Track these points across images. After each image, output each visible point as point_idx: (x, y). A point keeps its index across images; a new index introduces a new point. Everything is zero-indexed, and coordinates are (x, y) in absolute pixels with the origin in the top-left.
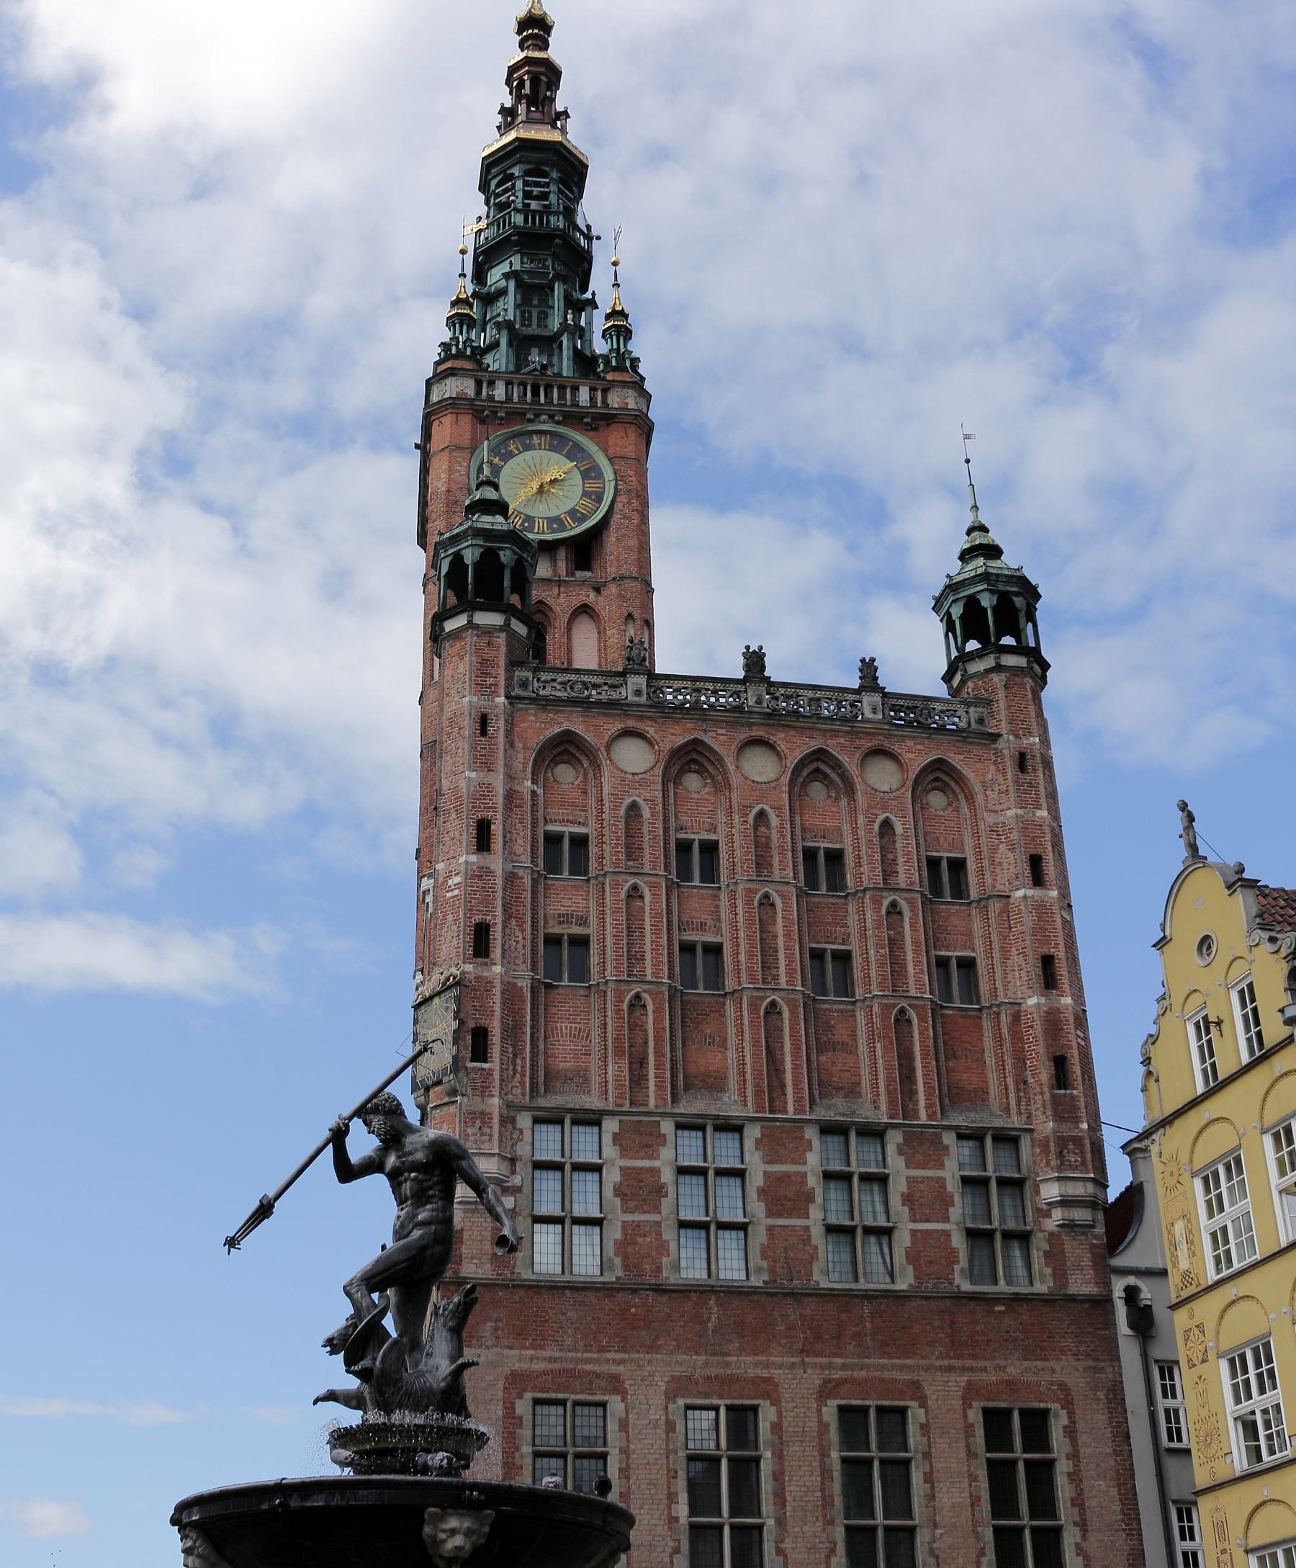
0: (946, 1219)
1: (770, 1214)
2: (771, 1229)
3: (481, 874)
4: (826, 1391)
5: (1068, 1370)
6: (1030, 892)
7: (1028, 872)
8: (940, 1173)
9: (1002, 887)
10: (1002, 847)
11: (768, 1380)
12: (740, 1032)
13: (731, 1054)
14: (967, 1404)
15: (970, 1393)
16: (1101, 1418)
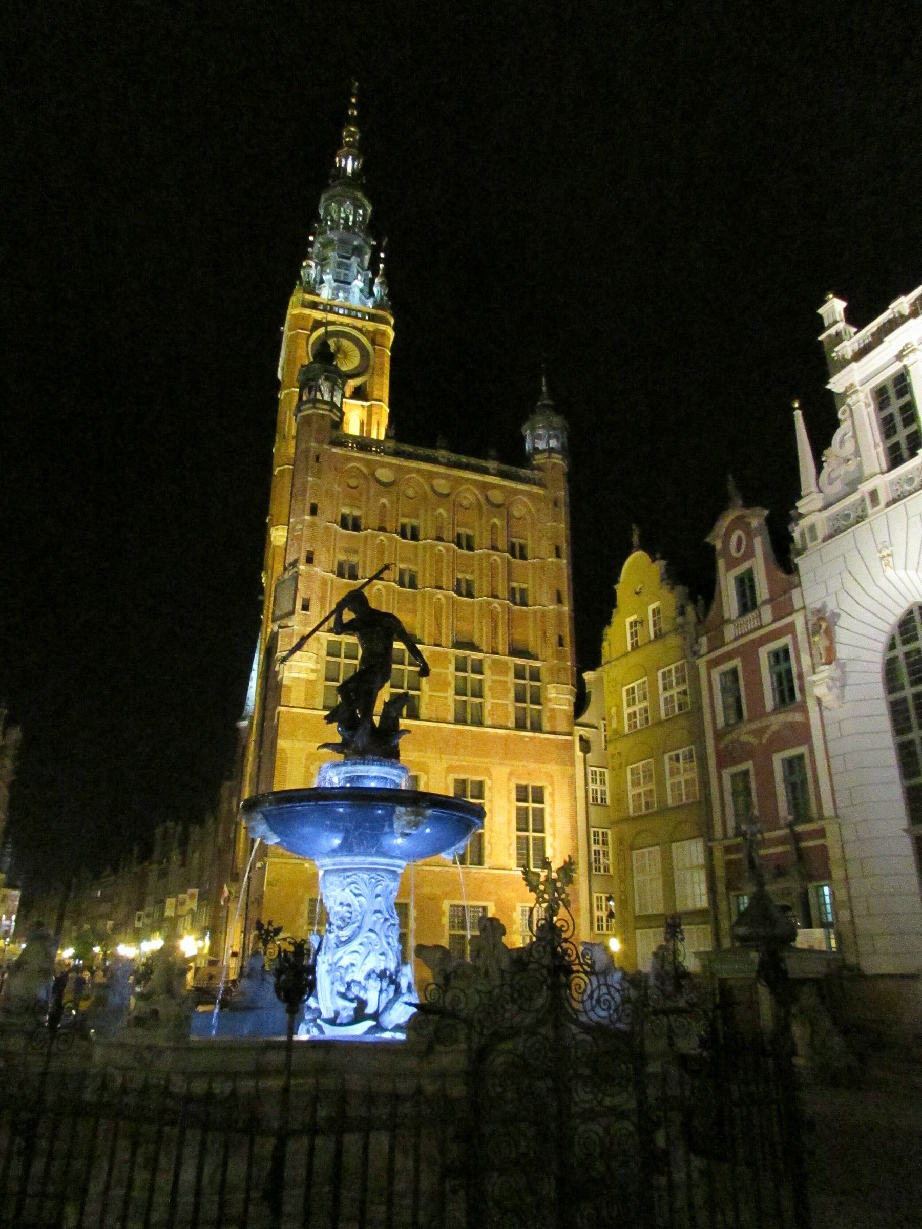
0: (506, 697)
1: (430, 690)
2: (431, 696)
3: (313, 525)
4: (450, 769)
5: (553, 768)
6: (554, 560)
7: (554, 552)
8: (505, 679)
9: (542, 554)
10: (545, 539)
11: (424, 764)
12: (424, 609)
13: (419, 618)
14: (509, 780)
15: (511, 774)
16: (565, 789)
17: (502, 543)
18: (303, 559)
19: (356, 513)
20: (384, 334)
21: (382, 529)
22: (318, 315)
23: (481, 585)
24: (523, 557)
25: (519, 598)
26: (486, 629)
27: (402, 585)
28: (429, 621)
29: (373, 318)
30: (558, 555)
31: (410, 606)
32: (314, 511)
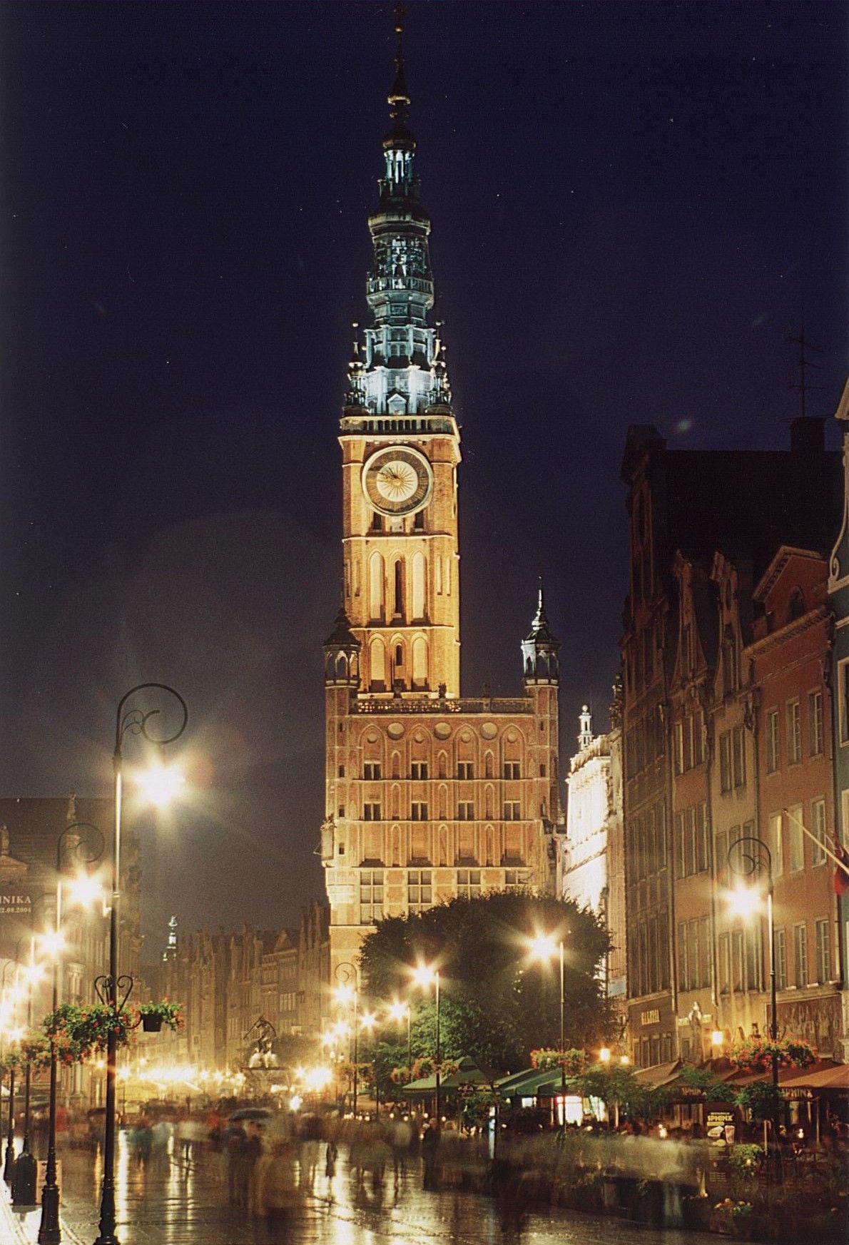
3: (341, 786)
9: (530, 775)
17: (495, 772)
18: (336, 814)
19: (377, 762)
20: (441, 444)
21: (396, 777)
22: (370, 438)
23: (479, 811)
24: (517, 776)
25: (512, 814)
26: (483, 846)
27: (414, 818)
28: (436, 849)
29: (426, 429)
30: (543, 775)
31: (421, 835)
32: (341, 774)
